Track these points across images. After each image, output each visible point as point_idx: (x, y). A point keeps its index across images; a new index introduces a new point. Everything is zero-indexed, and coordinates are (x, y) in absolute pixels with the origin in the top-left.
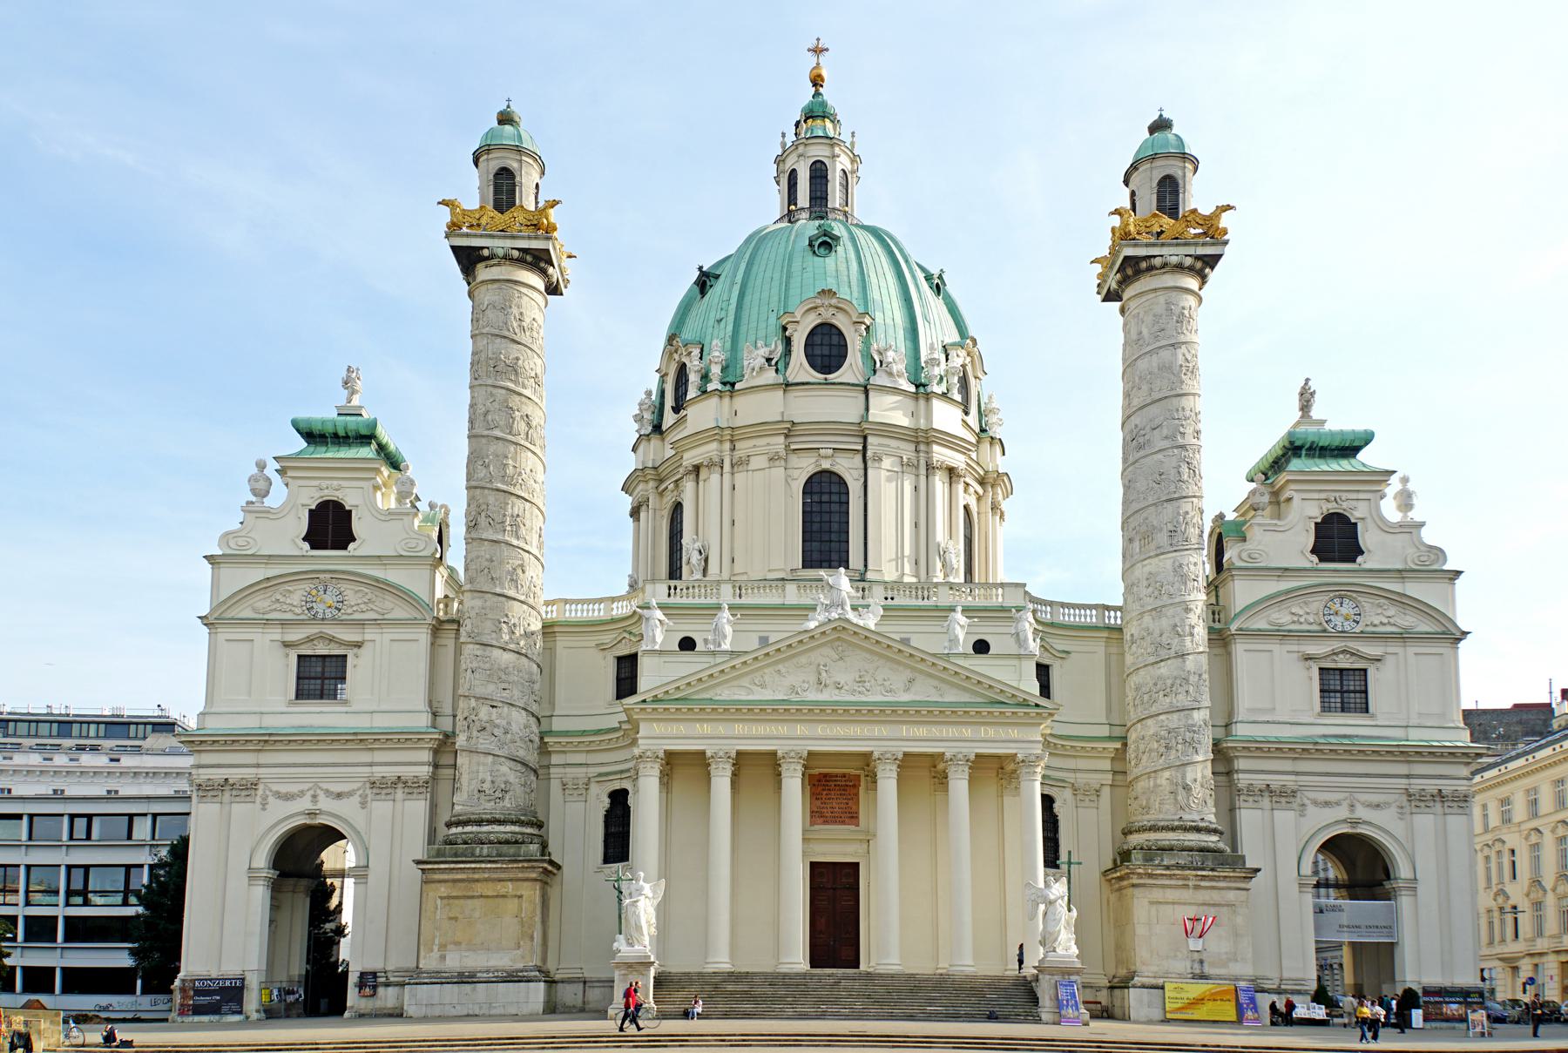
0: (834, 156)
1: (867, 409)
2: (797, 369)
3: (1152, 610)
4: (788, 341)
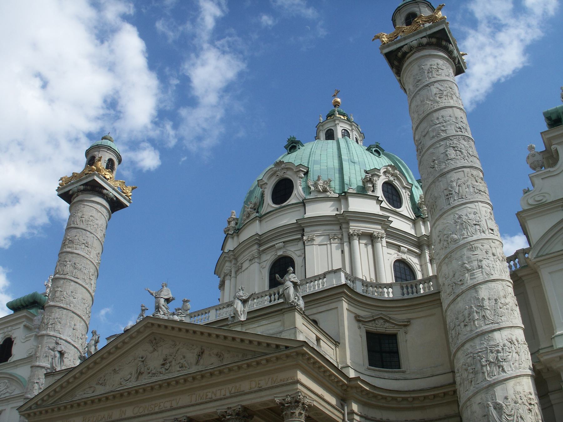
0: (336, 125)
1: (305, 214)
2: (267, 206)
3: (446, 257)
4: (262, 195)
